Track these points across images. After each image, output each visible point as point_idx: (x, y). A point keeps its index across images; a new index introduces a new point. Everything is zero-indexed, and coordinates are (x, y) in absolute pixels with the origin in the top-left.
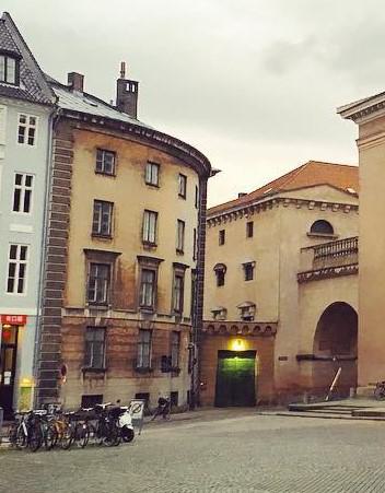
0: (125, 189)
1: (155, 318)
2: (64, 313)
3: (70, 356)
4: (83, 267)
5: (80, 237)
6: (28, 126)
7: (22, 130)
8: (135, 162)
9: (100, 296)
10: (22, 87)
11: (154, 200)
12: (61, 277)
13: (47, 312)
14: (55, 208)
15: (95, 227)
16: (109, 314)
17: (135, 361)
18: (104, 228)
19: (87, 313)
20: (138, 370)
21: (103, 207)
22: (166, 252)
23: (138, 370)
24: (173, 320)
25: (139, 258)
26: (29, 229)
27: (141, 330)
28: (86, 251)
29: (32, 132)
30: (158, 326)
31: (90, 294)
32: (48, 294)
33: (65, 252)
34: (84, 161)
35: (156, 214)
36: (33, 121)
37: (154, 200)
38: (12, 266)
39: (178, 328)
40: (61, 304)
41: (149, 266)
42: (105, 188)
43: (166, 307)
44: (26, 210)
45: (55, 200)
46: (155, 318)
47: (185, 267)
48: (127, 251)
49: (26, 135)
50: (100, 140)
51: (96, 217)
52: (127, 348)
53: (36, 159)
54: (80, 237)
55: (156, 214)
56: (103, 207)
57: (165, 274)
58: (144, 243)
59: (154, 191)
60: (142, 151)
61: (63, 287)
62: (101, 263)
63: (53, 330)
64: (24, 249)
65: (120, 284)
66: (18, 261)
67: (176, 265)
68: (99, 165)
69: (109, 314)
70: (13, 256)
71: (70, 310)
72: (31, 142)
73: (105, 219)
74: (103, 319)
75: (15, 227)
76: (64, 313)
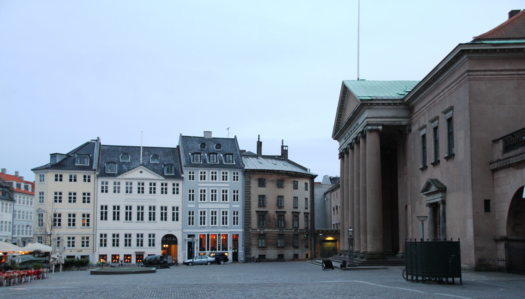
0: (270, 191)
1: (284, 230)
2: (251, 230)
3: (254, 243)
4: (256, 216)
5: (255, 207)
6: (236, 175)
7: (234, 177)
8: (272, 181)
9: (263, 224)
10: (234, 163)
11: (281, 192)
12: (249, 220)
13: (245, 230)
14: (246, 199)
15: (259, 203)
16: (266, 230)
17: (277, 244)
18: (263, 203)
19: (258, 230)
20: (279, 247)
21: (262, 198)
22: (288, 207)
23: (279, 247)
24: (293, 230)
25: (276, 212)
26: (238, 206)
27: (279, 235)
28: (257, 211)
29: (237, 177)
30: (286, 233)
31: (259, 224)
32: (246, 225)
33: (250, 212)
34: (254, 184)
35: (283, 196)
36: (237, 174)
37: (281, 192)
38: (234, 218)
39: (296, 233)
40: (249, 228)
41: (281, 215)
42: (262, 191)
43: (290, 226)
44: (237, 200)
45: (245, 197)
46: (284, 230)
47: (299, 213)
48: (271, 209)
49: (235, 178)
50: (259, 176)
51: (260, 200)
52: (273, 240)
53: (239, 185)
54: (255, 207)
55: (283, 196)
56: (262, 198)
57: (289, 217)
58: (278, 207)
59: (281, 190)
60: (275, 177)
61: (250, 223)
62: (262, 215)
63: (247, 235)
64: (237, 212)
65: (270, 221)
66: (236, 216)
67: (293, 212)
68: (259, 184)
69: (266, 230)
70: (234, 214)
71: (252, 229)
72: (237, 180)
73: (263, 200)
74: (264, 232)
75: (234, 206)
76: (251, 230)
